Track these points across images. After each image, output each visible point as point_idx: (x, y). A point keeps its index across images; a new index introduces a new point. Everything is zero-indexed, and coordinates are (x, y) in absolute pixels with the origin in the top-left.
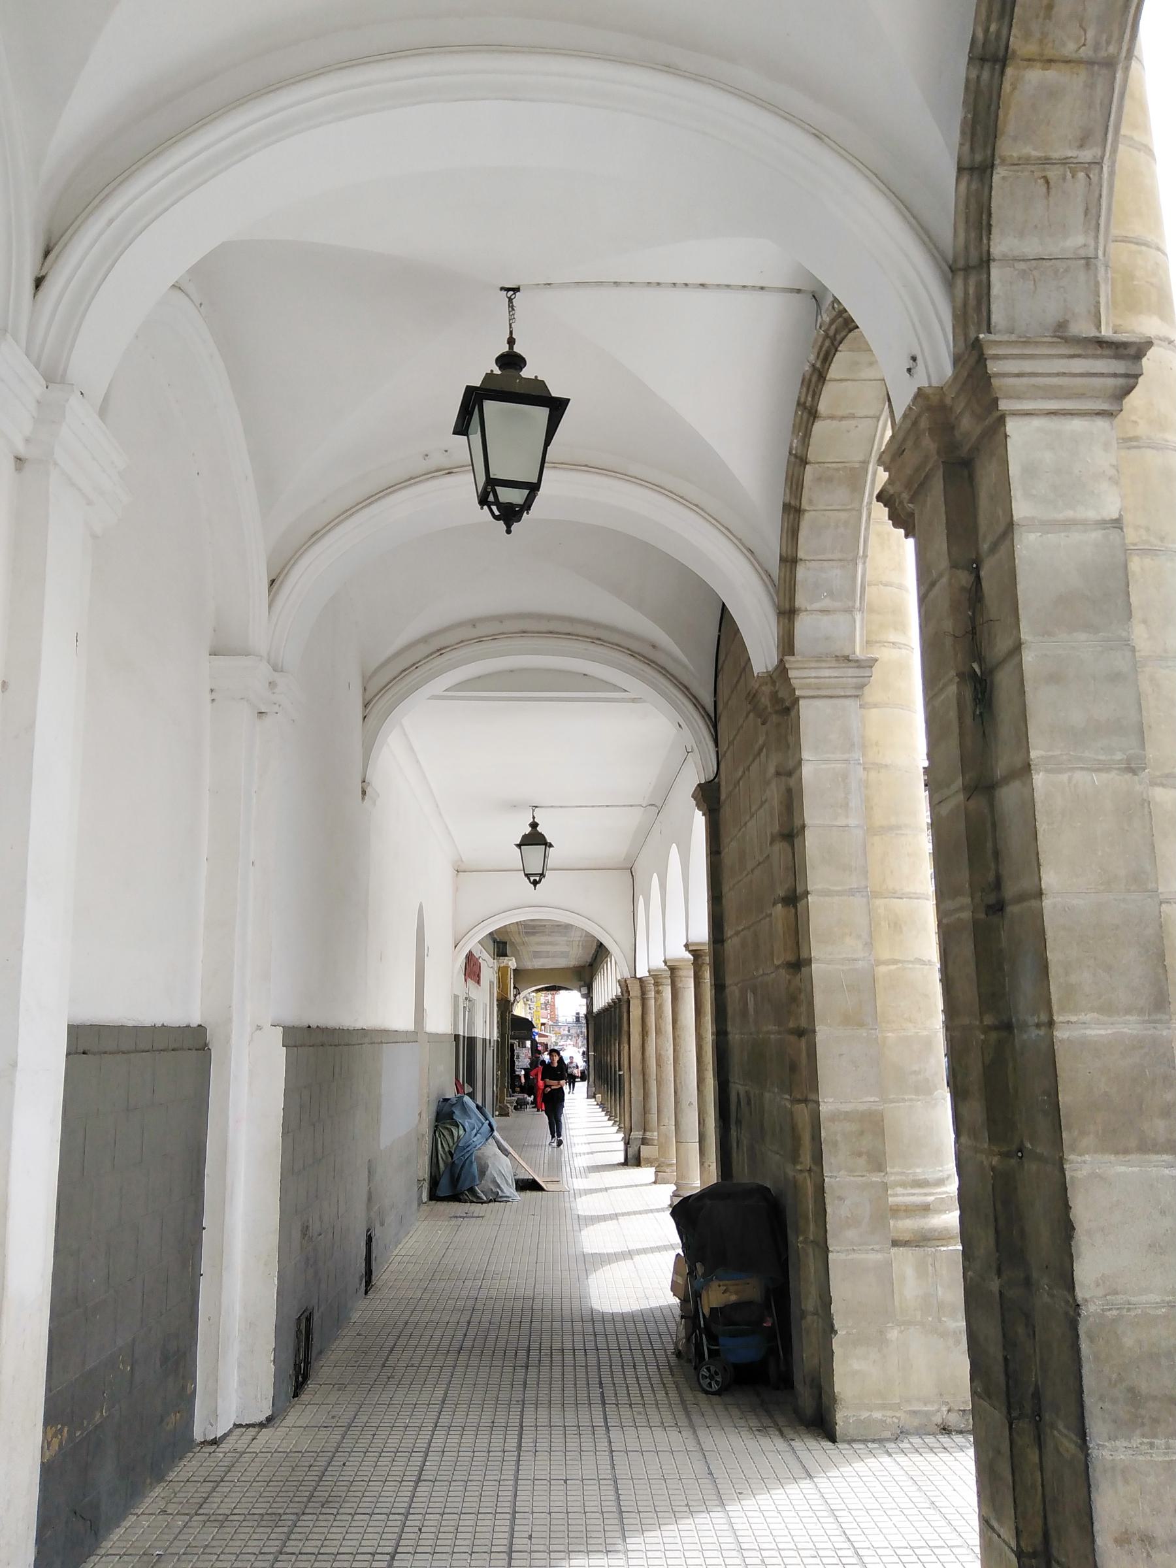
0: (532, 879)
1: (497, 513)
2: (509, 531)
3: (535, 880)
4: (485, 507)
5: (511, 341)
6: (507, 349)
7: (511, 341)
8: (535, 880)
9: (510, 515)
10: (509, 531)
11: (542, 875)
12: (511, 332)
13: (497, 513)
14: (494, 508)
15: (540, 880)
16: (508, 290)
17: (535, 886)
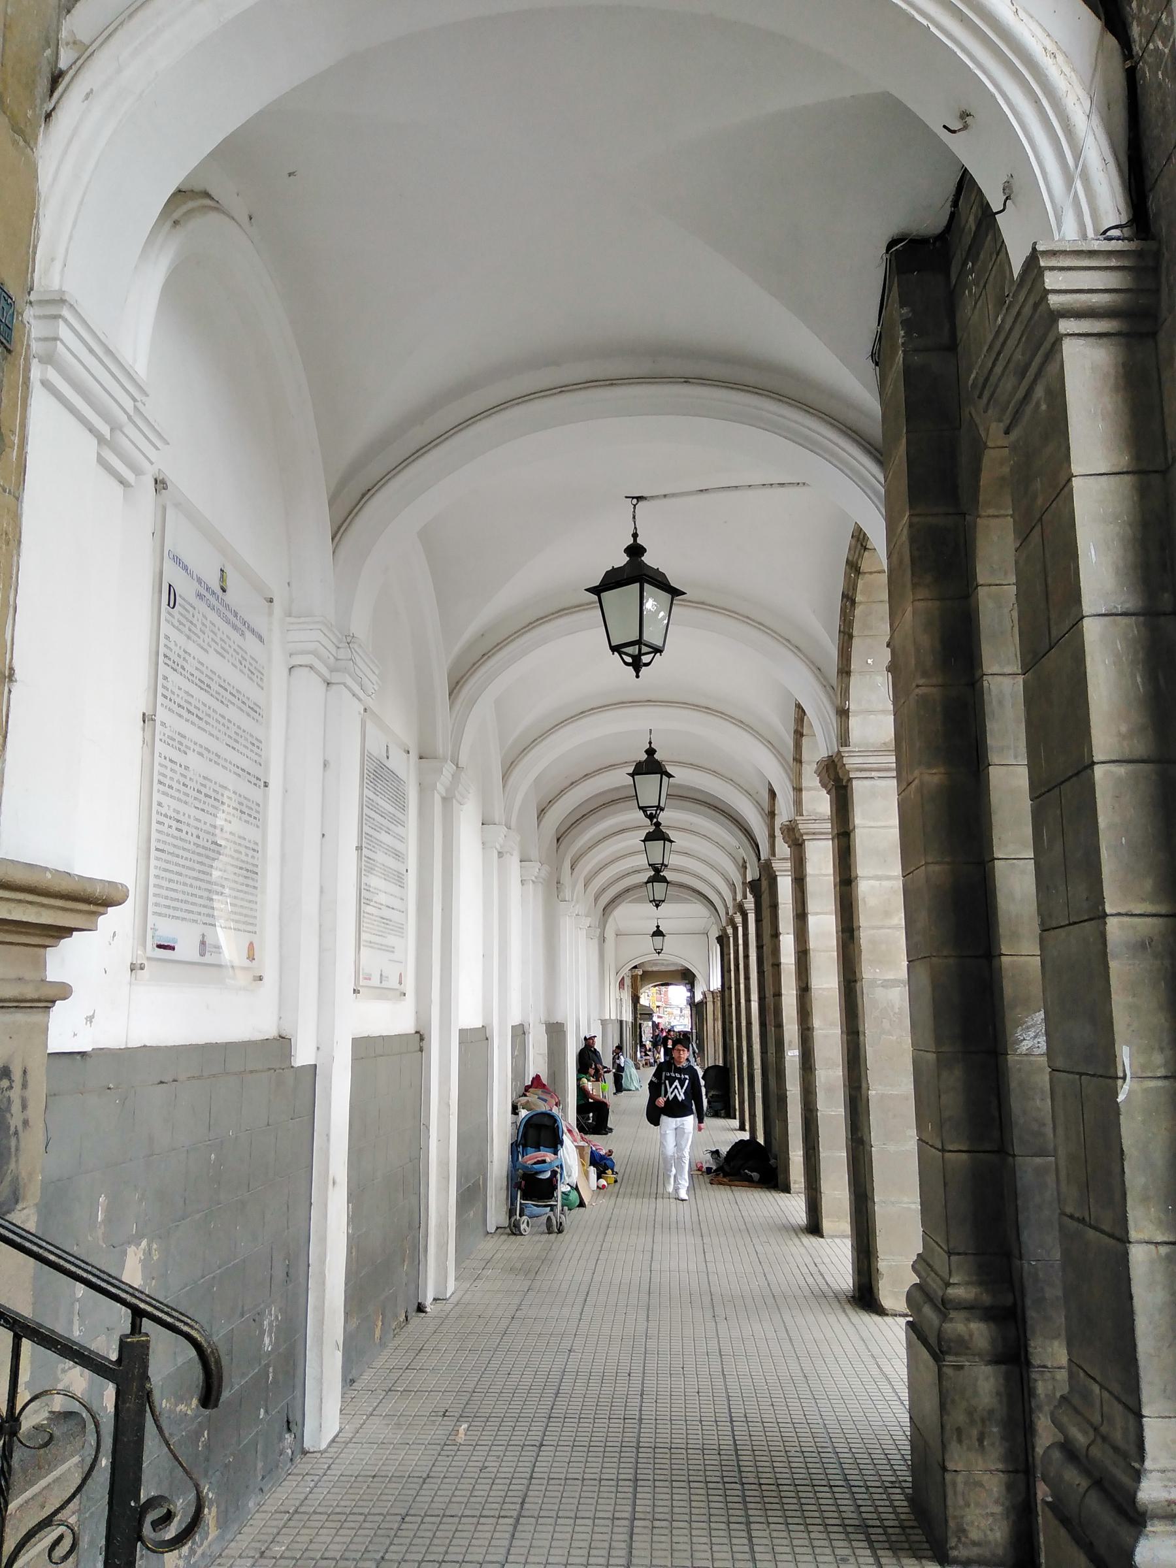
0: (649, 813)
2: (637, 676)
3: (651, 814)
5: (635, 536)
6: (632, 542)
7: (635, 536)
8: (651, 814)
10: (637, 676)
12: (635, 528)
16: (633, 498)
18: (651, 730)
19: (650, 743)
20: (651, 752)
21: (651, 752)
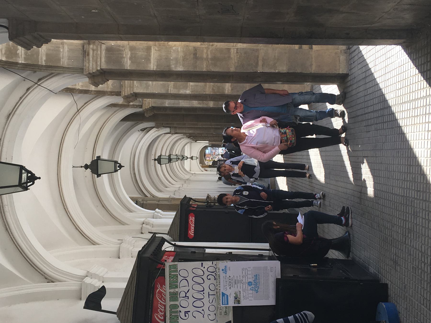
1: (32, 183)
2: (40, 178)
4: (28, 188)
9: (32, 178)
10: (40, 178)
11: (116, 162)
13: (32, 183)
14: (29, 184)
15: (119, 163)
17: (122, 167)
18: (74, 167)
19: (81, 167)
20: (86, 167)
21: (86, 167)
